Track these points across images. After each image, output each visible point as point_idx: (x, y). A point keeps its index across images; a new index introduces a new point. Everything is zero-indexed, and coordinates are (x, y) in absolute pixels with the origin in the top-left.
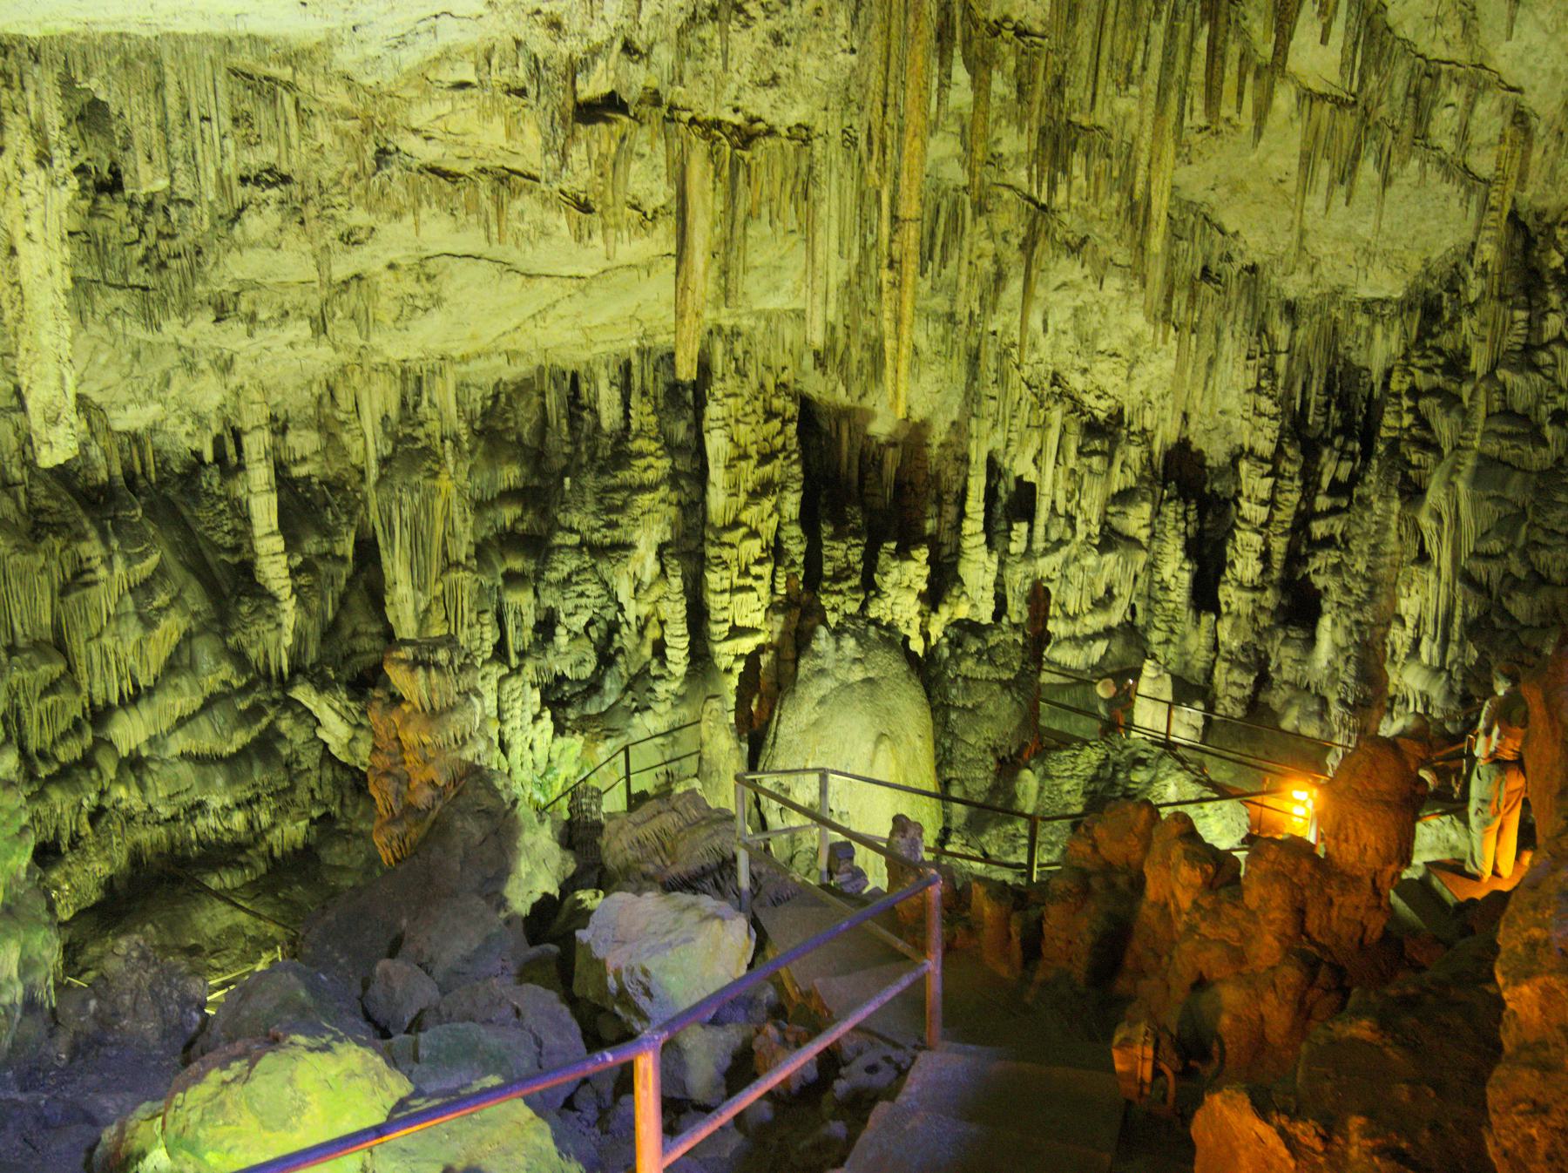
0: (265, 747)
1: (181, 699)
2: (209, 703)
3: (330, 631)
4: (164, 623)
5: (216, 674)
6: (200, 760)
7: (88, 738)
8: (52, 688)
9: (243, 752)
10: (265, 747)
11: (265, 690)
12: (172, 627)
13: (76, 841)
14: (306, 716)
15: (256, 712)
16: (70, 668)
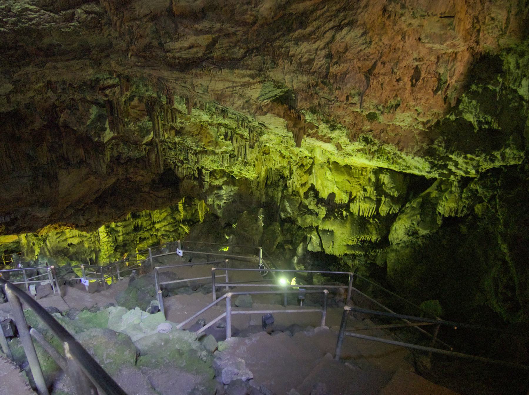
0: (176, 231)
1: (165, 223)
2: (169, 224)
3: (193, 215)
4: (163, 214)
5: (170, 220)
6: (166, 231)
7: (152, 226)
8: (147, 220)
9: (173, 231)
10: (176, 231)
11: (176, 223)
12: (164, 214)
13: (148, 238)
14: (181, 227)
15: (176, 226)
16: (151, 217)
